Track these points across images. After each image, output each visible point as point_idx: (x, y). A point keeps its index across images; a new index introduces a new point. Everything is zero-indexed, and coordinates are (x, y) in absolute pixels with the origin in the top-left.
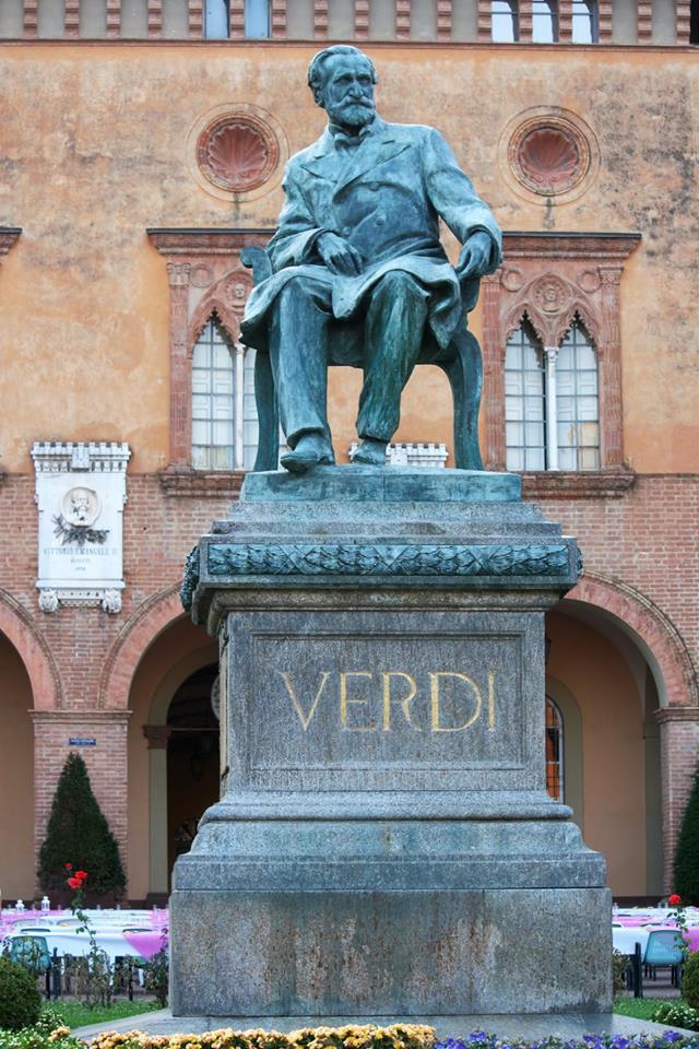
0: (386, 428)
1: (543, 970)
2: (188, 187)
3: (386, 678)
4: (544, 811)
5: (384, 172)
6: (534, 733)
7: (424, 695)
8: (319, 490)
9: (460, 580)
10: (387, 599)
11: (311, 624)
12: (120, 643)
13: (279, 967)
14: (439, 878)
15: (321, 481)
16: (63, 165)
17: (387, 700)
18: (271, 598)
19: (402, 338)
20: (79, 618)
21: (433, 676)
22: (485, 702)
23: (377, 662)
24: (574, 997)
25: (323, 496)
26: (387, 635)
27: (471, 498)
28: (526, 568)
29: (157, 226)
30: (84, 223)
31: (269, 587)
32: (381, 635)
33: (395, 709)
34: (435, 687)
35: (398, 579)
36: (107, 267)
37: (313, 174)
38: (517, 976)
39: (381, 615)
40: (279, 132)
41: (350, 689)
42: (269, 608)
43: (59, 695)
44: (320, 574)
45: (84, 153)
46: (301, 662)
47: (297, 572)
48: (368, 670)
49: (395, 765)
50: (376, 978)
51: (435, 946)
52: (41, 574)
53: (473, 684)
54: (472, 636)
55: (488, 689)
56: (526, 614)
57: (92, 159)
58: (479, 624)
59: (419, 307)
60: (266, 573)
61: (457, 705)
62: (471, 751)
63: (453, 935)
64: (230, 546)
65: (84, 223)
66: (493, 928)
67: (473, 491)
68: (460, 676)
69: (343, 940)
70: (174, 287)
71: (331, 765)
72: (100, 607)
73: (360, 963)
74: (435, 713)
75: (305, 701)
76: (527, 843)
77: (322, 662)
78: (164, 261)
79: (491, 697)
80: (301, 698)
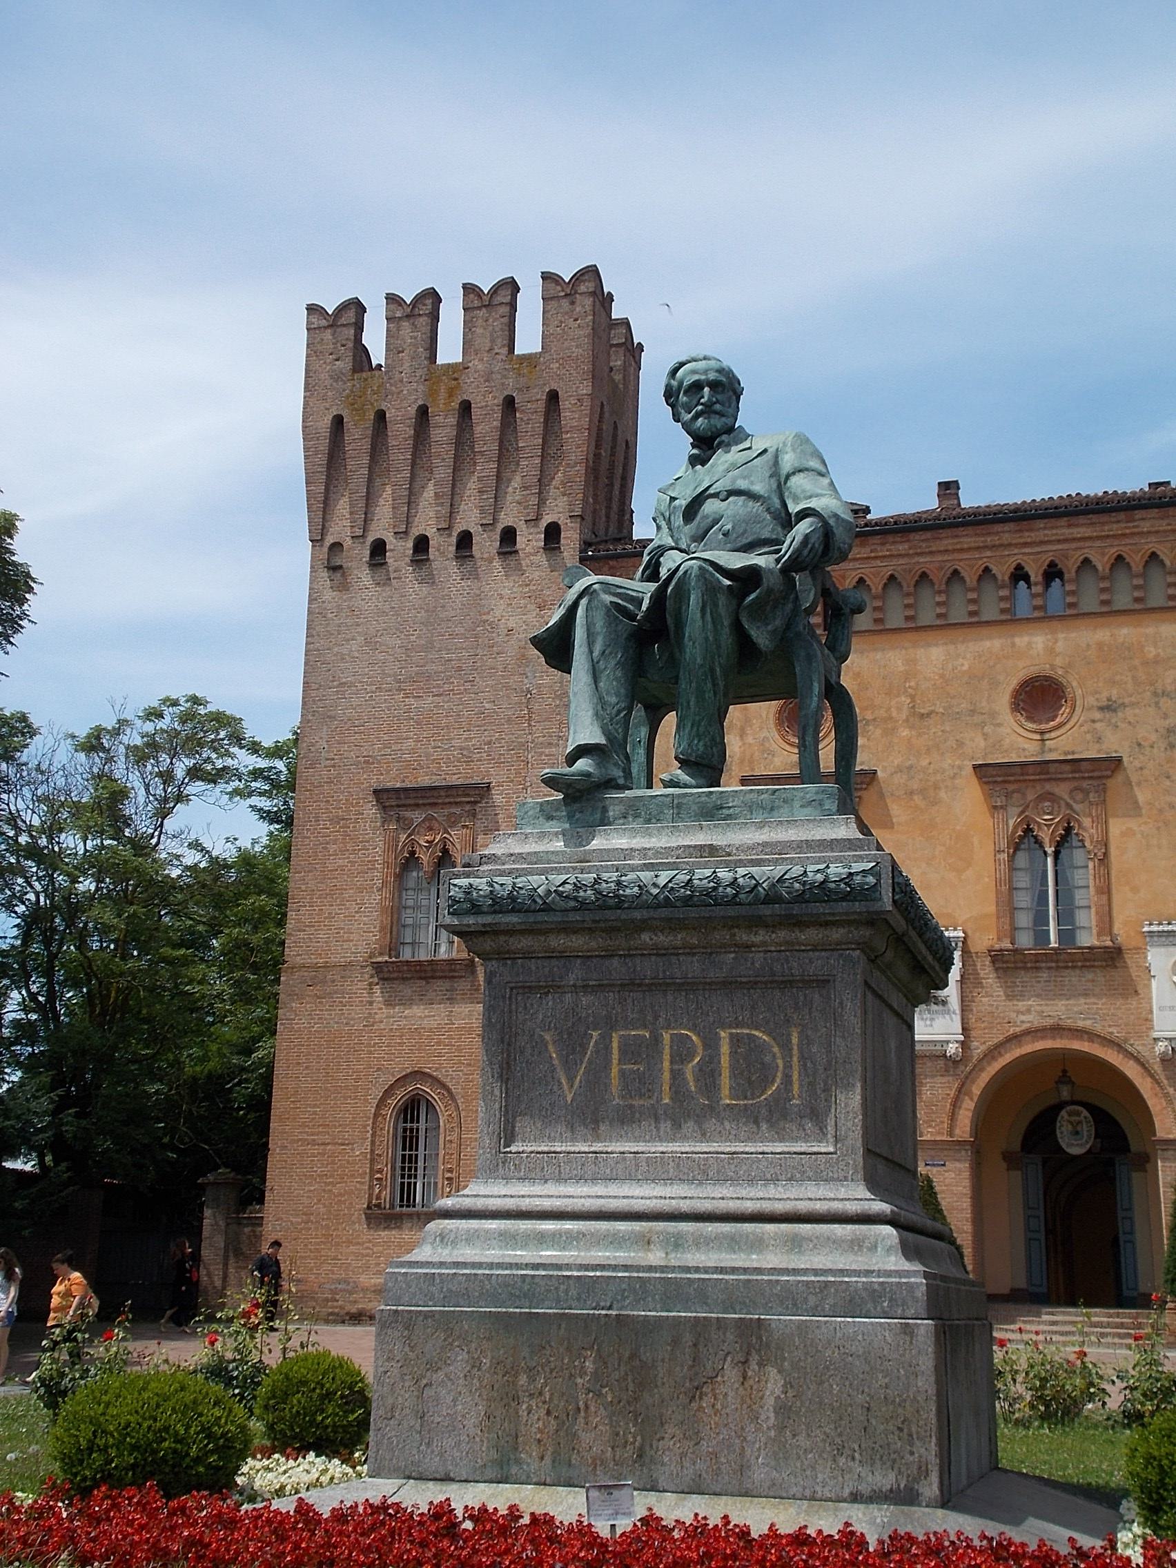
0: (702, 749)
1: (840, 1435)
2: (1004, 730)
3: (666, 1037)
4: (852, 1208)
5: (734, 480)
6: (846, 1105)
8: (598, 816)
9: (742, 911)
10: (662, 939)
13: (497, 1413)
15: (601, 805)
16: (907, 720)
17: (666, 1064)
18: (524, 942)
19: (707, 639)
20: (929, 1064)
21: (723, 1034)
22: (788, 1066)
23: (656, 1017)
24: (885, 1480)
26: (668, 984)
28: (823, 891)
30: (924, 763)
31: (518, 927)
32: (660, 985)
33: (676, 1075)
34: (725, 1049)
35: (664, 913)
36: (942, 794)
37: (673, 499)
38: (803, 1441)
39: (659, 959)
40: (1075, 684)
41: (623, 1051)
42: (528, 955)
44: (574, 909)
45: (922, 711)
47: (547, 908)
48: (645, 1027)
50: (617, 1434)
51: (695, 1394)
53: (772, 1043)
54: (771, 982)
55: (791, 1050)
56: (836, 954)
57: (929, 715)
58: (777, 967)
59: (722, 600)
60: (513, 910)
61: (753, 1070)
63: (719, 1378)
64: (471, 880)
65: (924, 763)
66: (772, 1372)
67: (779, 807)
68: (757, 1033)
69: (579, 1380)
70: (995, 807)
71: (598, 1147)
72: (945, 1055)
73: (599, 1416)
74: (725, 1081)
75: (570, 1068)
76: (826, 1256)
77: (591, 1019)
78: (986, 787)
79: (795, 1059)
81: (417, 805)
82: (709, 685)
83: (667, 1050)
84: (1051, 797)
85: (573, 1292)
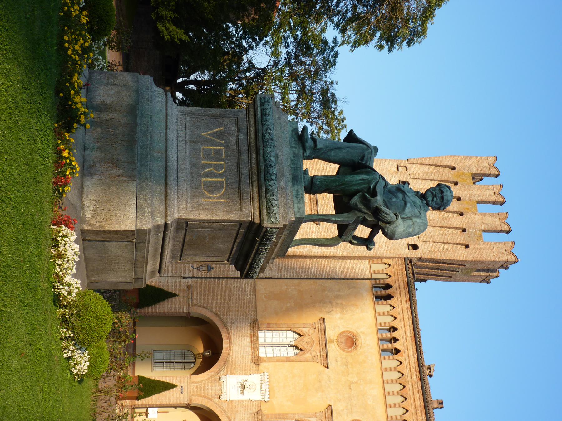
7: (216, 176)
8: (293, 145)
10: (254, 160)
11: (242, 137)
12: (211, 400)
14: (142, 165)
17: (214, 162)
20: (219, 388)
22: (214, 198)
23: (229, 160)
25: (291, 147)
27: (295, 198)
29: (333, 408)
33: (210, 165)
34: (219, 179)
35: (262, 159)
36: (320, 394)
43: (196, 383)
44: (263, 133)
46: (227, 134)
49: (188, 164)
52: (231, 376)
58: (245, 195)
59: (366, 186)
60: (262, 115)
62: (194, 192)
70: (316, 413)
75: (213, 134)
78: (323, 410)
80: (214, 133)
81: (310, 199)
82: (338, 184)
83: (218, 163)
85: (143, 128)
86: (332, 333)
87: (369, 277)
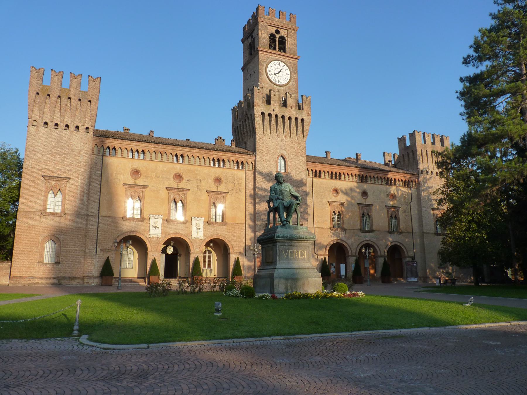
84: (179, 194)
86: (131, 181)
87: (101, 157)
